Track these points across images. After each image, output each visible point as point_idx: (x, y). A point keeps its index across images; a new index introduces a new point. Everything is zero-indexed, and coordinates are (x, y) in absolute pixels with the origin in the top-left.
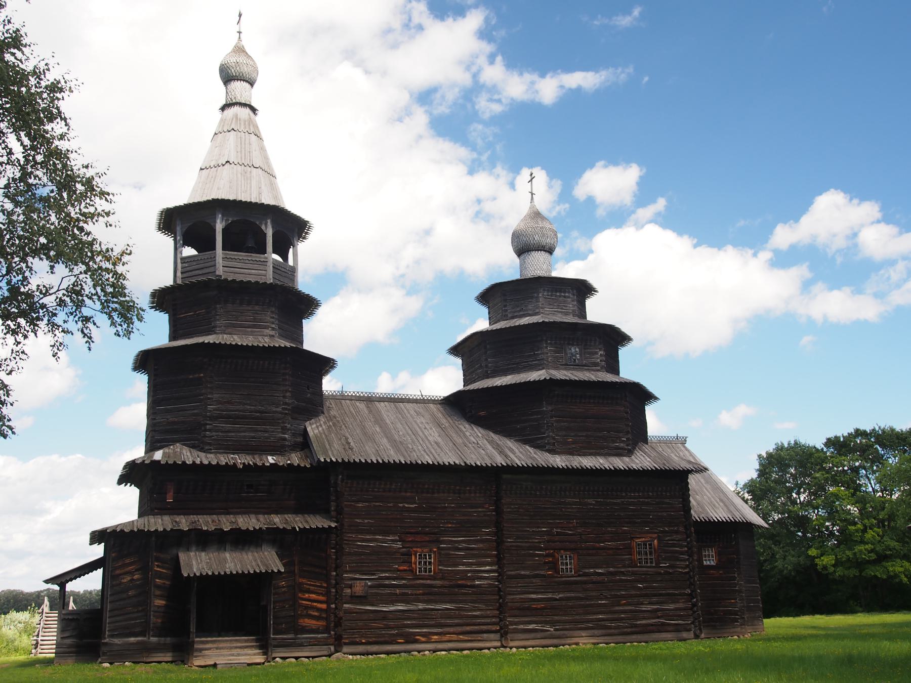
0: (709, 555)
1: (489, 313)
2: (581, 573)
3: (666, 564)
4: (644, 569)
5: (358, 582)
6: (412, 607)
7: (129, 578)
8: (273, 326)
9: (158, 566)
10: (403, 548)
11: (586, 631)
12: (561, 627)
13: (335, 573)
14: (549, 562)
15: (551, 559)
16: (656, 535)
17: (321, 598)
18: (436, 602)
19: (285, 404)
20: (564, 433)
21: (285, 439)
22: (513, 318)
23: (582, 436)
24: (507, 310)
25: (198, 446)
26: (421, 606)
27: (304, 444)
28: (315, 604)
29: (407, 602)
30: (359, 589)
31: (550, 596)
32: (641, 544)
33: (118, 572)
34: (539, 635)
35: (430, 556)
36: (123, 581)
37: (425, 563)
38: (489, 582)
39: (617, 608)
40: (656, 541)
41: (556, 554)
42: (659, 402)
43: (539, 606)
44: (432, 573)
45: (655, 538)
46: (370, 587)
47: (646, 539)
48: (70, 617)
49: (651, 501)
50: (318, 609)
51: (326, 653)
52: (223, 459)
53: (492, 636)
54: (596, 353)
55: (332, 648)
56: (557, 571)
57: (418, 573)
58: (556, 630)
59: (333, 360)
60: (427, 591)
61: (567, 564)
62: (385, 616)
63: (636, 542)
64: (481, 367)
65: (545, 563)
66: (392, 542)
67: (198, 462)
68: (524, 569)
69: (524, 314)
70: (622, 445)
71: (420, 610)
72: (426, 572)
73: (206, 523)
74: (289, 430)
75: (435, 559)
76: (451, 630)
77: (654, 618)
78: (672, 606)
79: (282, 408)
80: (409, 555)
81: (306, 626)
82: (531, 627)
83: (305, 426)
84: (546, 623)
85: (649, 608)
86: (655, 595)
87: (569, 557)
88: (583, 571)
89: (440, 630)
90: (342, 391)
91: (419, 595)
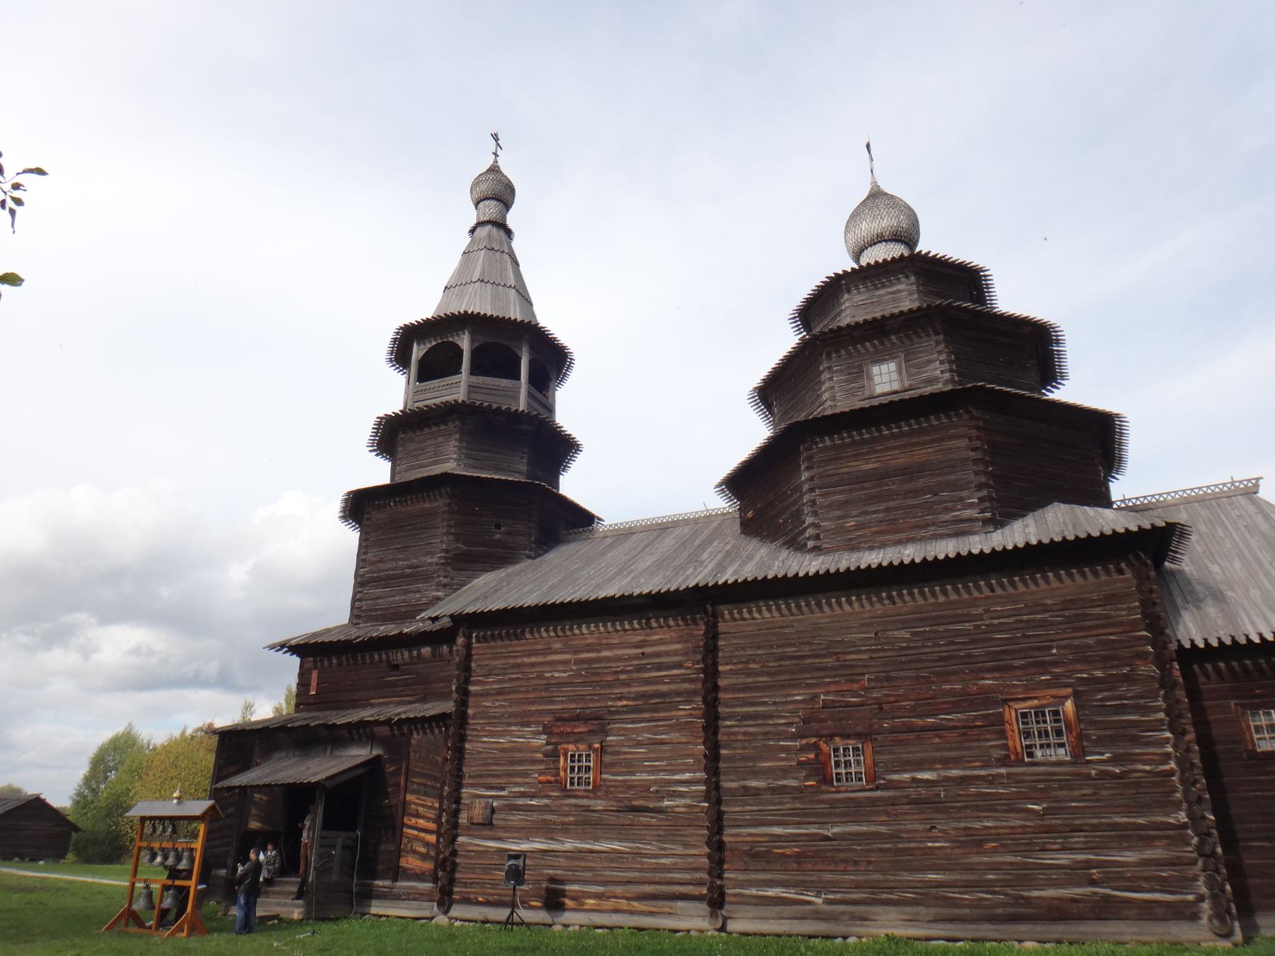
2: (882, 782)
3: (1102, 754)
5: (477, 801)
10: (547, 744)
14: (808, 762)
16: (1070, 690)
20: (838, 513)
23: (875, 512)
28: (423, 835)
31: (813, 830)
32: (1030, 713)
35: (589, 755)
41: (823, 745)
43: (788, 851)
44: (591, 787)
45: (1066, 698)
47: (1043, 702)
49: (1051, 616)
56: (827, 780)
57: (568, 787)
58: (829, 902)
61: (847, 764)
63: (1016, 710)
65: (800, 763)
75: (596, 762)
76: (619, 890)
81: (408, 869)
82: (771, 892)
85: (1064, 859)
87: (856, 749)
88: (888, 777)
89: (601, 889)
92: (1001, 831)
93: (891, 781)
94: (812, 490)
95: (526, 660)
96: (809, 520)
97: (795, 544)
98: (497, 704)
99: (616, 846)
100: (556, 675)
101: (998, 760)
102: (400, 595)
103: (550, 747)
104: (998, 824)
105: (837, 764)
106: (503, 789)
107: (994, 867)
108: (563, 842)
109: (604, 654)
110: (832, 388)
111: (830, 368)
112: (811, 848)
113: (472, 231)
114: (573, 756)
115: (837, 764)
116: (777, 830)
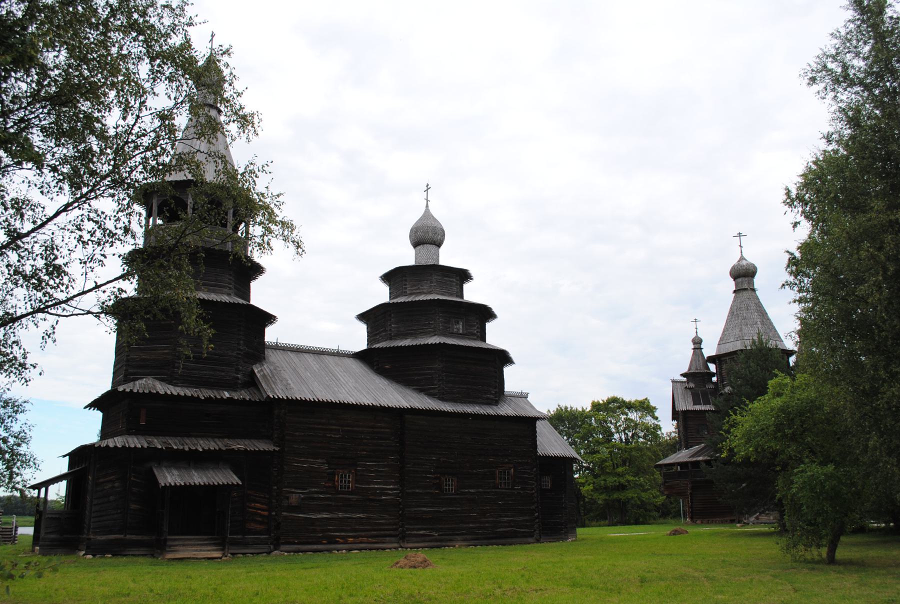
0: (546, 481)
1: (390, 289)
4: (504, 490)
5: (294, 495)
7: (110, 486)
8: (231, 286)
9: (134, 477)
10: (328, 469)
12: (443, 533)
13: (276, 488)
15: (438, 481)
17: (264, 507)
19: (240, 350)
21: (238, 378)
22: (411, 294)
24: (406, 288)
25: (170, 380)
26: (341, 515)
27: (252, 382)
28: (259, 511)
30: (294, 499)
33: (101, 480)
34: (428, 538)
35: (349, 476)
36: (105, 488)
37: (345, 481)
38: (392, 497)
40: (512, 470)
41: (443, 479)
42: (513, 366)
45: (511, 468)
46: (302, 499)
48: (54, 516)
50: (261, 515)
51: (266, 550)
52: (188, 392)
53: (393, 539)
54: (474, 326)
55: (272, 547)
59: (275, 317)
62: (313, 521)
64: (385, 331)
66: (321, 465)
67: (169, 393)
69: (420, 293)
70: (492, 396)
71: (340, 518)
72: (345, 488)
73: (175, 444)
74: (240, 371)
75: (352, 479)
76: (363, 534)
77: (508, 527)
78: (521, 518)
79: (237, 353)
80: (333, 474)
82: (422, 532)
83: (252, 369)
84: (432, 530)
85: (506, 519)
87: (452, 480)
90: (277, 343)
95: (316, 426)
97: (431, 395)
98: (301, 447)
100: (333, 436)
105: (446, 485)
106: (306, 489)
107: (487, 522)
109: (355, 429)
114: (342, 475)
115: (446, 485)
116: (425, 509)
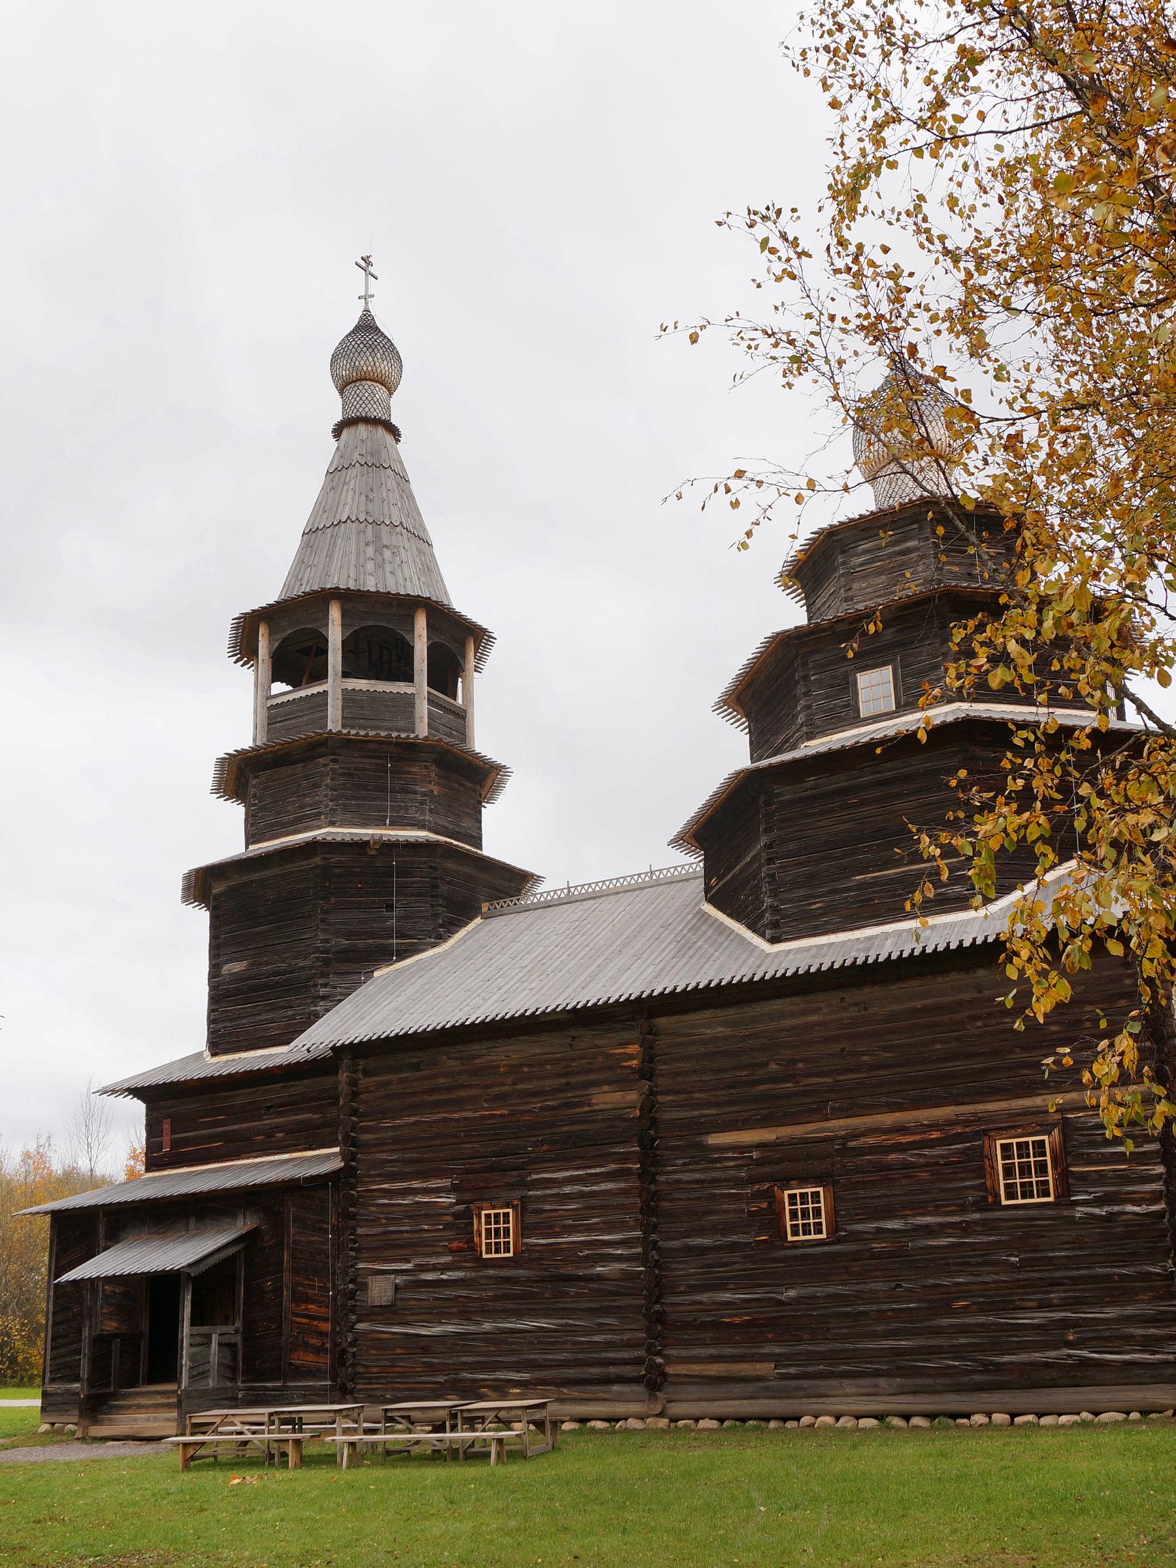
2: (843, 1233)
6: (473, 1328)
10: (457, 1203)
11: (852, 1381)
15: (764, 1205)
18: (519, 1314)
20: (801, 892)
26: (487, 1326)
28: (315, 1323)
29: (465, 1314)
30: (380, 1291)
39: (945, 1321)
43: (737, 1320)
46: (397, 1288)
60: (499, 1293)
62: (423, 1345)
68: (701, 1232)
80: (467, 1215)
81: (302, 1366)
85: (1038, 1317)
86: (1056, 1283)
88: (849, 1228)
89: (526, 1376)
91: (485, 1300)
92: (974, 1287)
93: (852, 1233)
94: (770, 861)
96: (768, 901)
99: (542, 1323)
101: (975, 1203)
102: (269, 1011)
103: (462, 1207)
104: (970, 1279)
108: (478, 1323)
110: (809, 707)
111: (806, 678)
112: (762, 1316)
113: (338, 431)
